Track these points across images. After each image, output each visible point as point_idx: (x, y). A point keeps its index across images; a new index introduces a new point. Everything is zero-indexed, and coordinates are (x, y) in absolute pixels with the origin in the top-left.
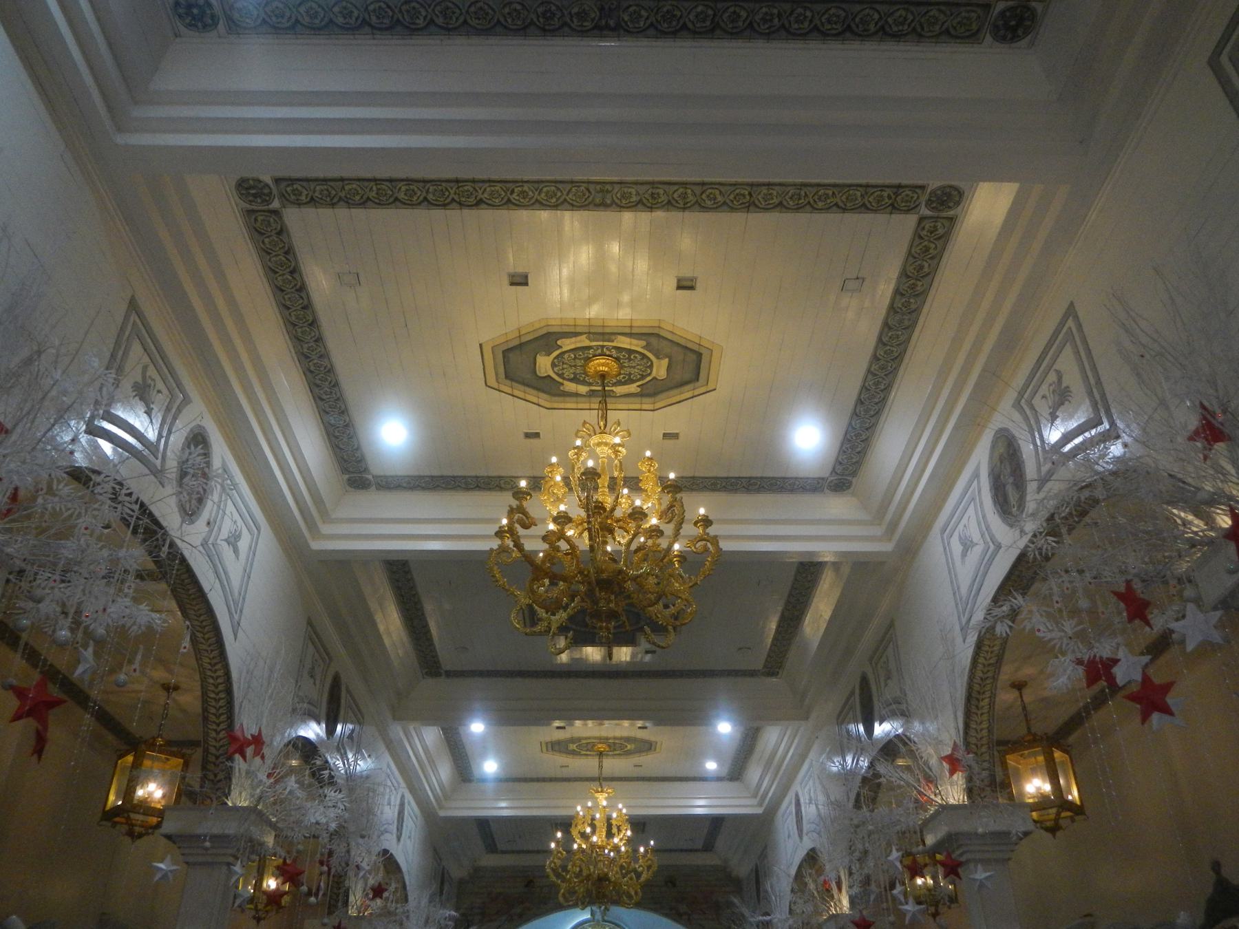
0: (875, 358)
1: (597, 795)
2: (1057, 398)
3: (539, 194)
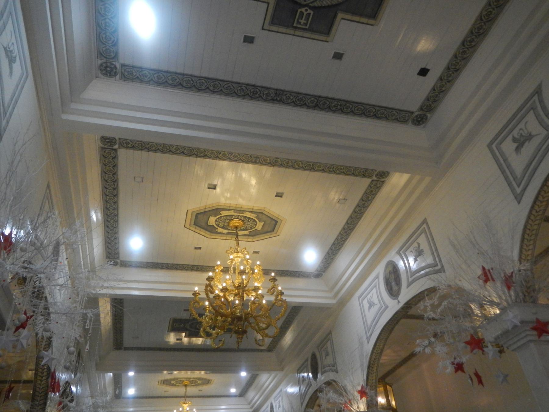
0: (344, 228)
1: (184, 405)
2: (417, 253)
3: (231, 156)
